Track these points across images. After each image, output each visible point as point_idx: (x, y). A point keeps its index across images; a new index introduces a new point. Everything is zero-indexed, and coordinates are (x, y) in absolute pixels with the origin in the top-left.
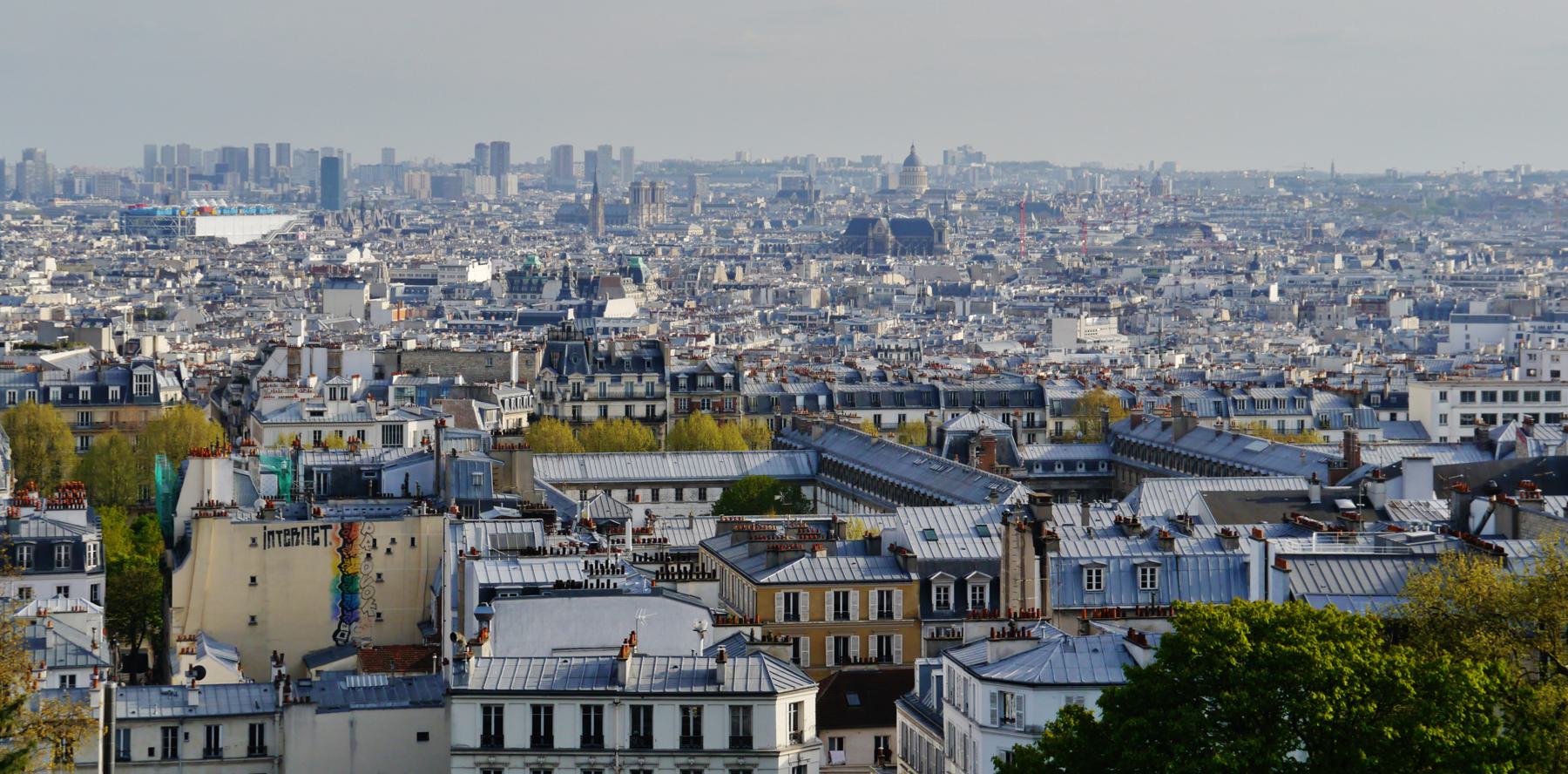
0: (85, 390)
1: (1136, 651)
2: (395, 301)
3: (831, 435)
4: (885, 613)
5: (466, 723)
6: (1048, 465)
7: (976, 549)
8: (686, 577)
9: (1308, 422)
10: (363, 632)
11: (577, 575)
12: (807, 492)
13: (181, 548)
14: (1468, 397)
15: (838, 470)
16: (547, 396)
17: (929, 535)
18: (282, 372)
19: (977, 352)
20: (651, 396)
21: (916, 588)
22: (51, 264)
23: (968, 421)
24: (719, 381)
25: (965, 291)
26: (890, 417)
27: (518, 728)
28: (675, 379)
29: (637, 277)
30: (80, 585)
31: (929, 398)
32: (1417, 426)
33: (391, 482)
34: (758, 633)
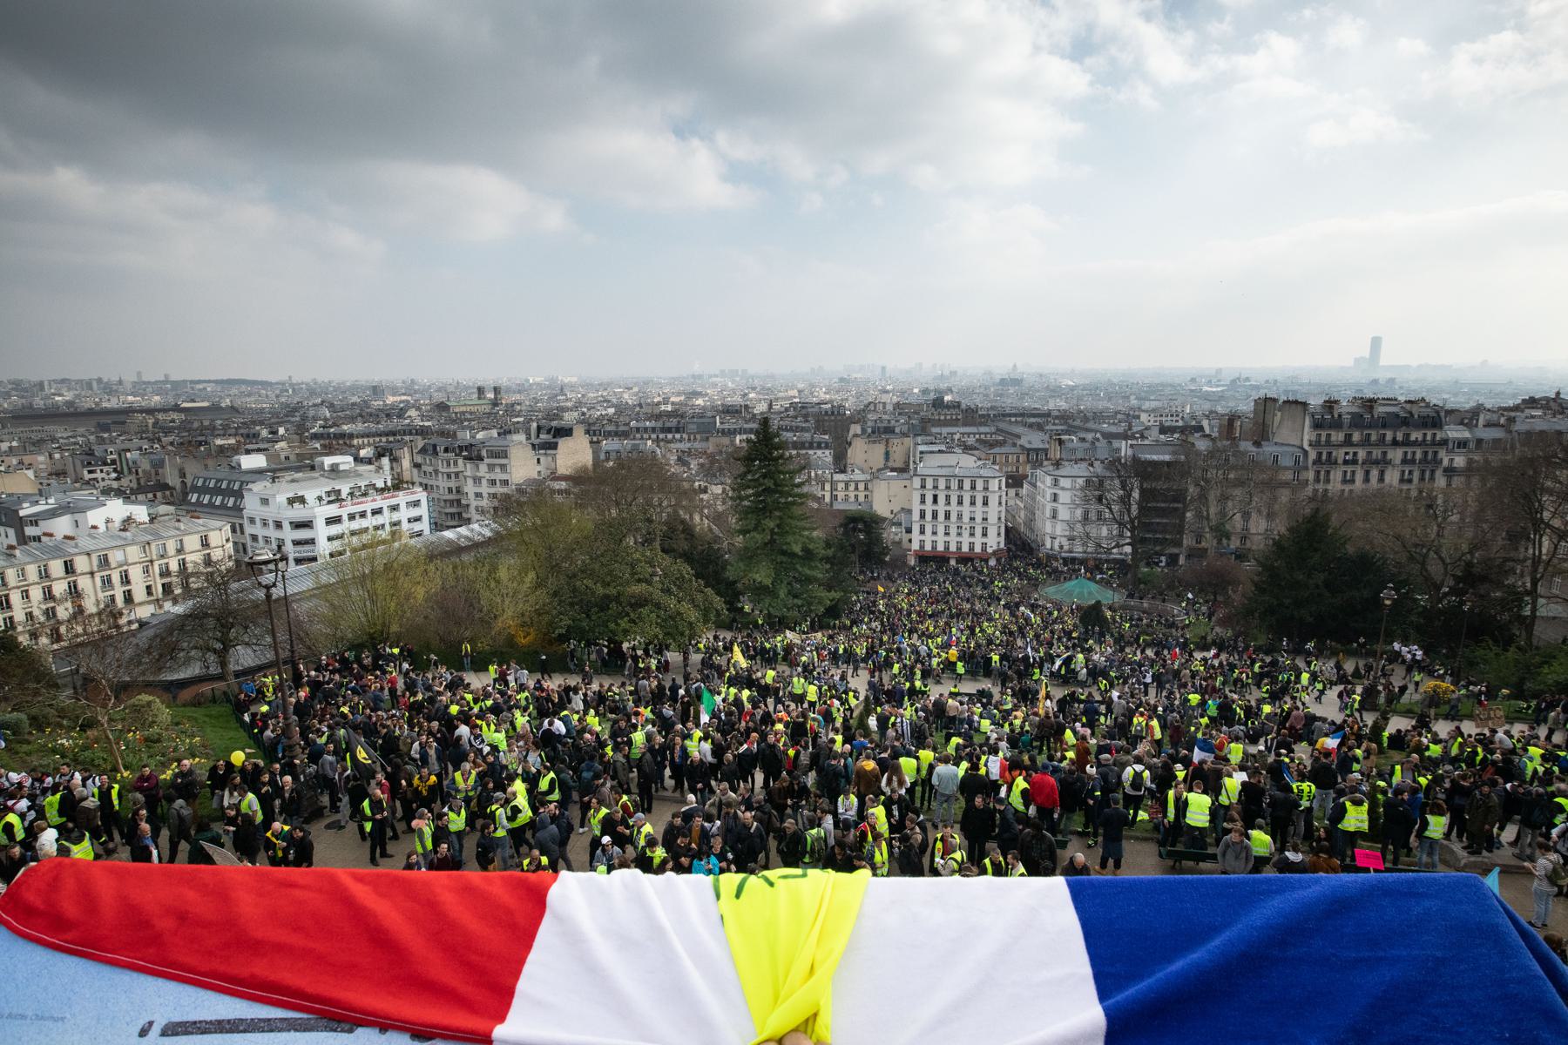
1: (1091, 468)
4: (1018, 461)
5: (917, 482)
7: (1041, 446)
8: (971, 449)
10: (890, 464)
11: (944, 449)
13: (850, 444)
15: (1002, 431)
16: (933, 414)
17: (1030, 443)
20: (957, 414)
23: (1032, 420)
26: (1013, 419)
30: (827, 452)
32: (1143, 423)
33: (897, 430)
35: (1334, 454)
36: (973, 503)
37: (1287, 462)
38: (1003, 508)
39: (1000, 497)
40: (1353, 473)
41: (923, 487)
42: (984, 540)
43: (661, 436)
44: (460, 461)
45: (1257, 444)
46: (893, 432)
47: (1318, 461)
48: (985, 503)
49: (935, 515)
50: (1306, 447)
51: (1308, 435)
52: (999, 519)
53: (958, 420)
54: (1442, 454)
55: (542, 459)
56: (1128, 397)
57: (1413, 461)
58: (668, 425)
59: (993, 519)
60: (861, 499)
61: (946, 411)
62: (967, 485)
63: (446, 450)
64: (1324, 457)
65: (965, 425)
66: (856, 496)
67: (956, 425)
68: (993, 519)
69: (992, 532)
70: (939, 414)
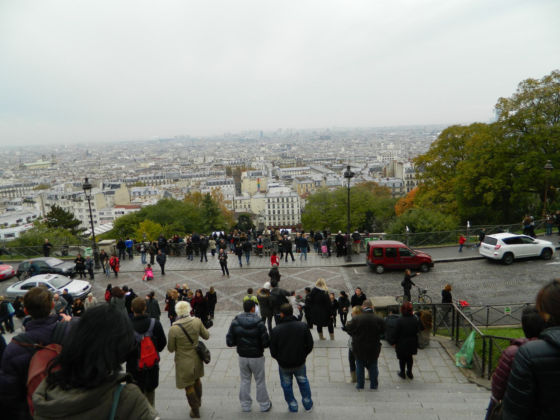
0: (233, 163)
2: (268, 149)
3: (312, 165)
5: (266, 200)
6: (336, 167)
8: (288, 185)
11: (278, 185)
12: (309, 171)
13: (242, 181)
14: (383, 157)
19: (333, 152)
21: (314, 183)
24: (300, 159)
26: (319, 162)
27: (271, 200)
29: (295, 144)
30: (232, 186)
31: (323, 160)
33: (263, 174)
34: (294, 190)
35: (413, 182)
36: (288, 207)
37: (397, 185)
38: (299, 208)
39: (298, 204)
41: (269, 201)
42: (293, 221)
43: (154, 181)
44: (70, 202)
45: (388, 179)
46: (261, 175)
48: (293, 207)
49: (274, 212)
50: (404, 180)
51: (405, 175)
52: (298, 212)
53: (294, 163)
55: (108, 199)
58: (157, 175)
59: (296, 212)
60: (247, 206)
61: (288, 160)
62: (285, 200)
63: (63, 198)
65: (298, 166)
66: (245, 206)
67: (293, 167)
68: (296, 212)
70: (285, 161)
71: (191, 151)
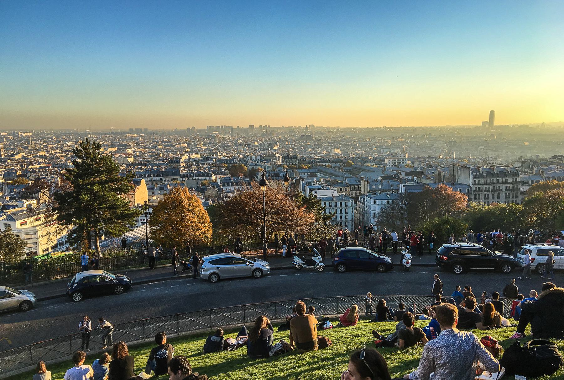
7: (356, 183)
9: (374, 164)
14: (393, 160)
15: (322, 171)
18: (249, 159)
21: (349, 187)
22: (202, 143)
24: (304, 160)
25: (318, 145)
28: (298, 159)
36: (341, 213)
39: (352, 209)
40: (488, 195)
47: (475, 191)
48: (346, 213)
52: (352, 218)
54: (519, 186)
56: (372, 146)
57: (509, 190)
59: (349, 218)
64: (478, 189)
68: (349, 218)
69: (350, 224)
70: (287, 162)
71: (156, 146)
